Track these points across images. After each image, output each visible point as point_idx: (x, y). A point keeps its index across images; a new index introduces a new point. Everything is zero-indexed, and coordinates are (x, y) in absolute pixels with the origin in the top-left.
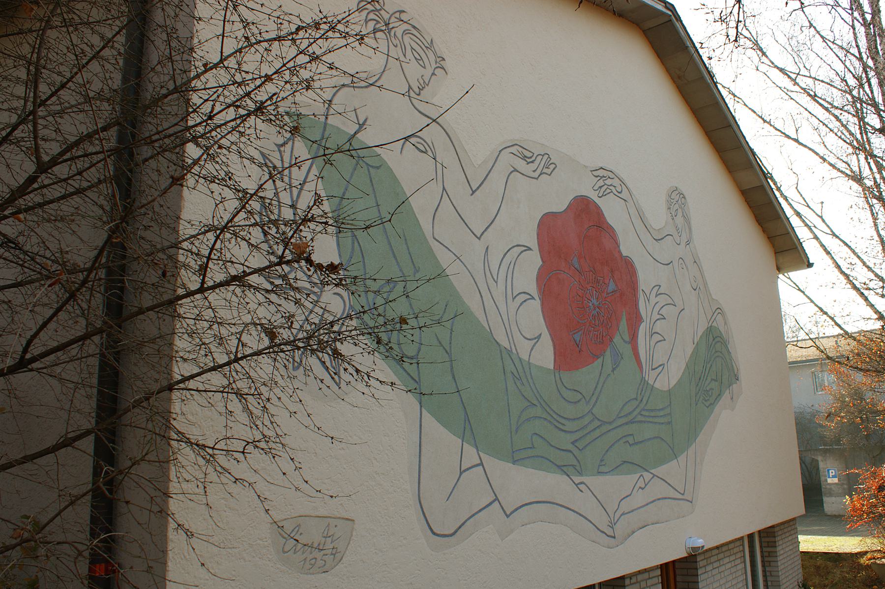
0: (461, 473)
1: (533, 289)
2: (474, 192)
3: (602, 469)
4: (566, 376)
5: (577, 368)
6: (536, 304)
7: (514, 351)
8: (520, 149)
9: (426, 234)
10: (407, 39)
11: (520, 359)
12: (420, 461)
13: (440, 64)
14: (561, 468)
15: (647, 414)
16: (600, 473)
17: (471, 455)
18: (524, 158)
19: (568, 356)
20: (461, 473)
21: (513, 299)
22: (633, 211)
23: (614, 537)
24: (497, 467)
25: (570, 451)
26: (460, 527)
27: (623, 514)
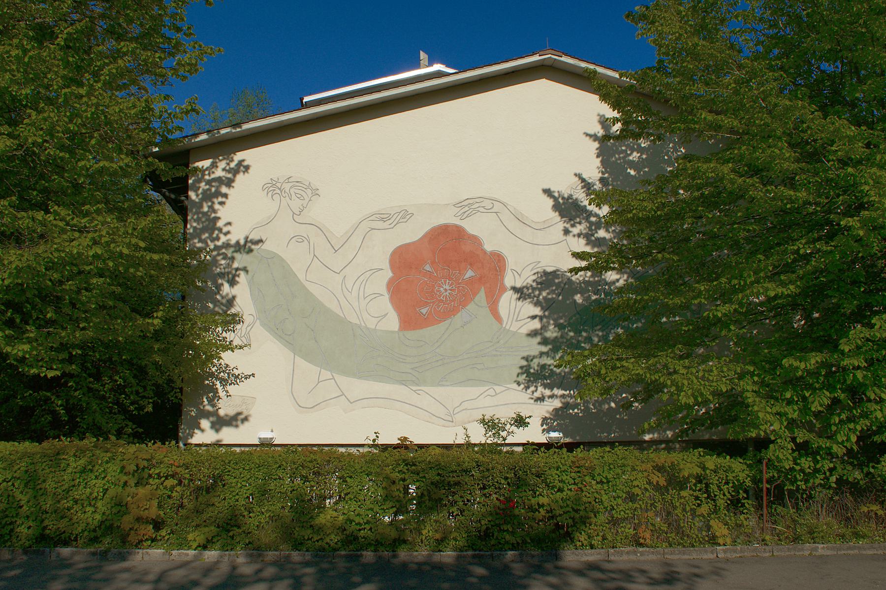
1: (384, 290)
4: (410, 334)
10: (292, 191)
13: (316, 193)
14: (403, 382)
18: (382, 220)
24: (342, 380)
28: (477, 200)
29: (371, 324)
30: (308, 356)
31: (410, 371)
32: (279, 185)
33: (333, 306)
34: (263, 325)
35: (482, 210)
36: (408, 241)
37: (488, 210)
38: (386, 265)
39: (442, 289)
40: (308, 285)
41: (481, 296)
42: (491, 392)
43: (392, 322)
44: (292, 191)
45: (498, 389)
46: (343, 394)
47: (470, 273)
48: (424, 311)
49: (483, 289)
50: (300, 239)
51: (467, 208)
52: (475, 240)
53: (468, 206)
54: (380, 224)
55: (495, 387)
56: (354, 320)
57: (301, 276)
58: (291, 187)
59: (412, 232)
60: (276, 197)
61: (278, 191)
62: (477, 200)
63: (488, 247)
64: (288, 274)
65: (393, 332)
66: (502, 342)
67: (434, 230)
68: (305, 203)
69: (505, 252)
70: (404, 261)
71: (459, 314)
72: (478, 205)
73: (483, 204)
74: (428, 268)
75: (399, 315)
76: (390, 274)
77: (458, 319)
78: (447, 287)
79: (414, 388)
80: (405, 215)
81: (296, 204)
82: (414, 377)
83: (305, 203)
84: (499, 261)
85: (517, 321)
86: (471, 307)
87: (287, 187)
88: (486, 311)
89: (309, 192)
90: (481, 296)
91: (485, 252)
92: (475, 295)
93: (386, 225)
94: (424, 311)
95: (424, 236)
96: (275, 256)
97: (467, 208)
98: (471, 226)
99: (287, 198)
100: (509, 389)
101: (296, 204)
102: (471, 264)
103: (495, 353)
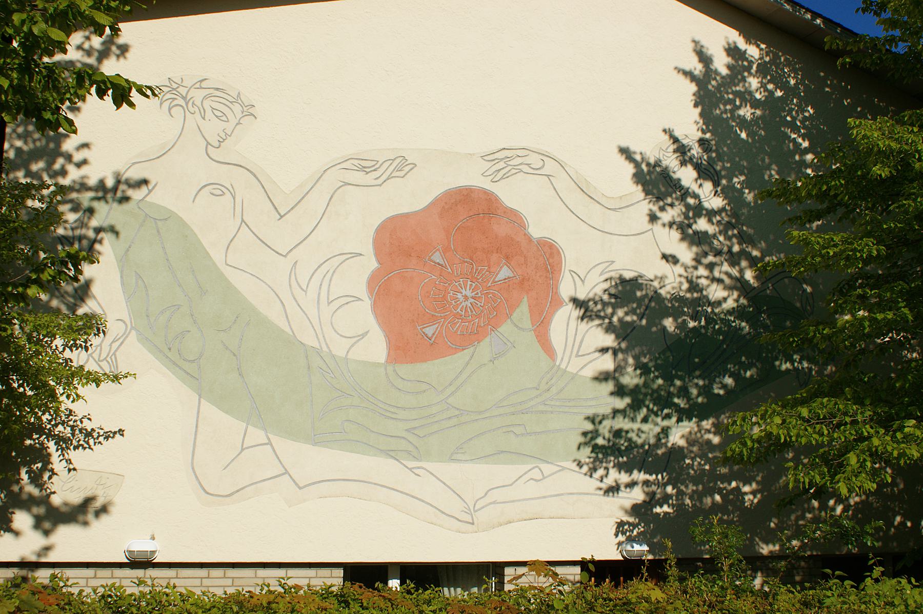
0: (243, 449)
1: (361, 290)
2: (282, 217)
3: (459, 456)
4: (405, 370)
5: (425, 361)
6: (367, 303)
7: (325, 349)
8: (356, 162)
9: (218, 265)
10: (207, 104)
11: (333, 356)
12: (195, 438)
13: (249, 112)
14: (389, 453)
15: (552, 403)
16: (452, 460)
17: (256, 435)
18: (363, 169)
19: (404, 348)
20: (243, 449)
21: (329, 303)
22: (562, 182)
23: (473, 524)
25: (403, 438)
26: (238, 491)
27: (494, 503)
28: (520, 153)
29: (339, 348)
30: (223, 402)
31: (404, 434)
32: (183, 91)
33: (273, 313)
34: (144, 340)
35: (526, 169)
36: (405, 210)
37: (536, 171)
38: (368, 249)
39: (459, 296)
40: (229, 273)
41: (523, 313)
42: (536, 474)
43: (376, 347)
44: (207, 104)
45: (547, 468)
46: (287, 472)
47: (505, 272)
48: (429, 331)
49: (525, 299)
50: (218, 189)
51: (502, 165)
52: (514, 217)
53: (505, 161)
54: (358, 177)
55: (543, 466)
56: (310, 340)
57: (217, 256)
58: (205, 98)
59: (413, 196)
60: (177, 111)
61: (183, 103)
62: (520, 153)
63: (536, 232)
64: (193, 249)
65: (377, 365)
66: (554, 390)
67: (448, 194)
68: (229, 127)
69: (561, 241)
70: (397, 242)
71: (487, 340)
72: (519, 161)
73: (527, 160)
74: (437, 258)
75: (387, 336)
76: (374, 265)
77: (485, 348)
78: (469, 293)
79: (411, 464)
80: (402, 166)
81: (213, 128)
82: (409, 447)
83: (229, 127)
84: (551, 254)
85: (577, 356)
86: (506, 328)
87: (197, 95)
88: (530, 338)
89: (237, 108)
90: (523, 313)
91: (529, 239)
92: (513, 308)
93: (369, 179)
94: (429, 331)
95: (433, 204)
96: (169, 216)
97: (502, 165)
98: (512, 194)
99: (197, 115)
100: (563, 468)
101: (213, 128)
102: (507, 258)
103: (541, 408)
